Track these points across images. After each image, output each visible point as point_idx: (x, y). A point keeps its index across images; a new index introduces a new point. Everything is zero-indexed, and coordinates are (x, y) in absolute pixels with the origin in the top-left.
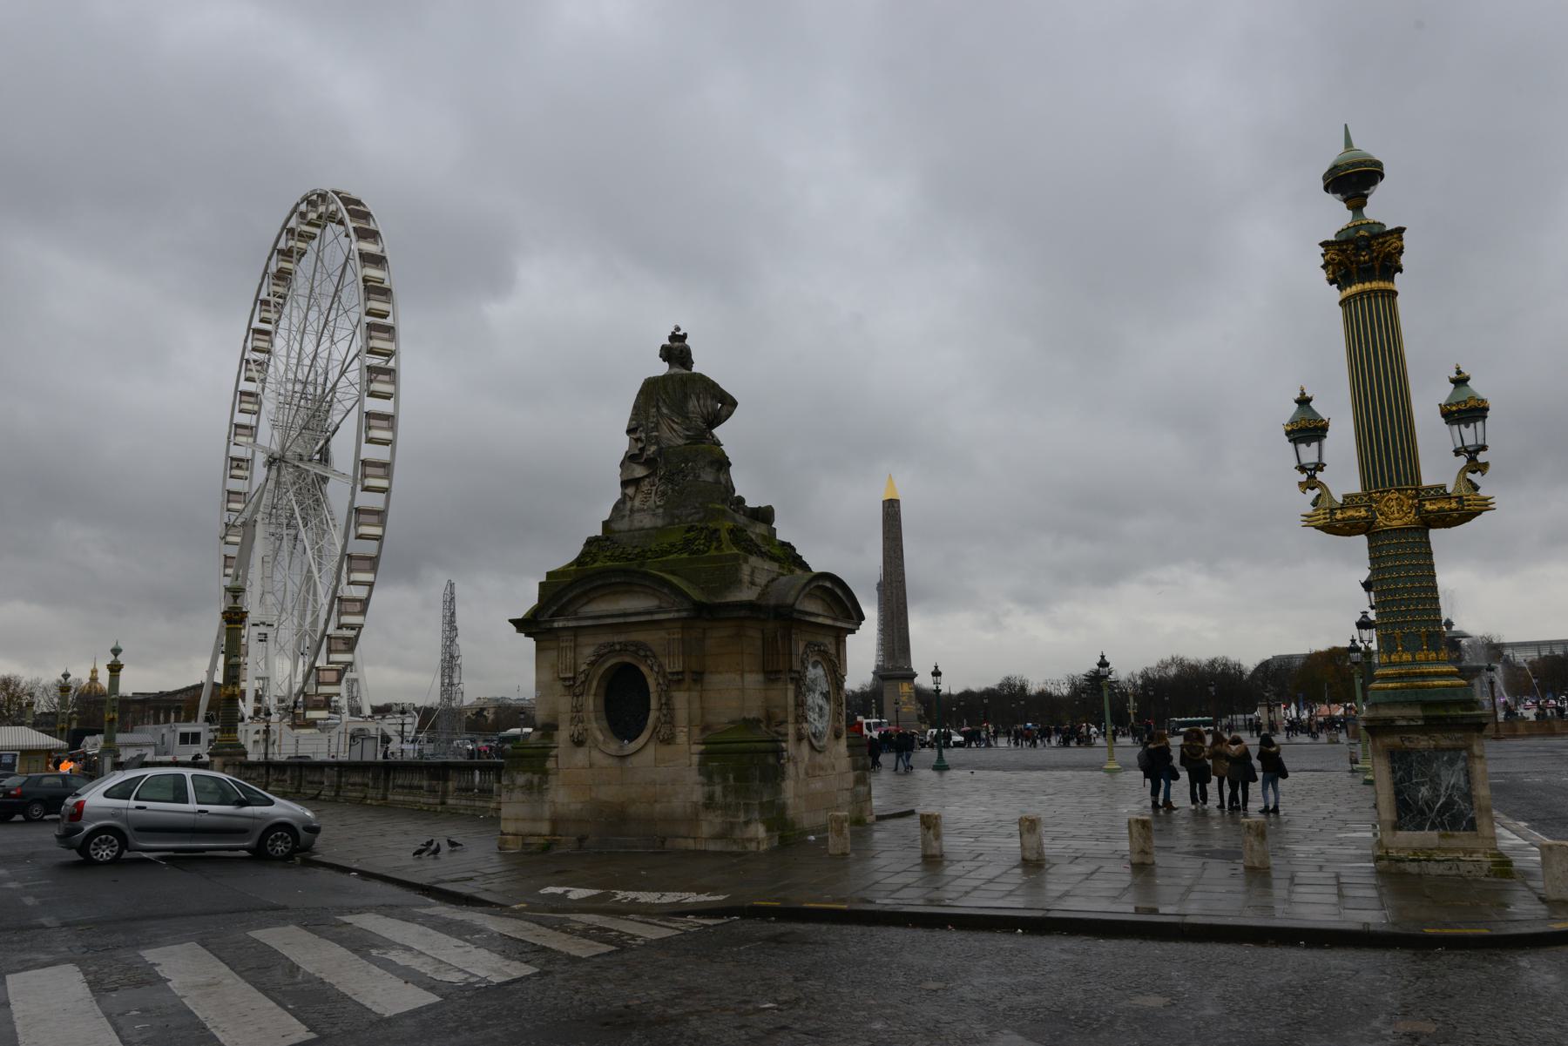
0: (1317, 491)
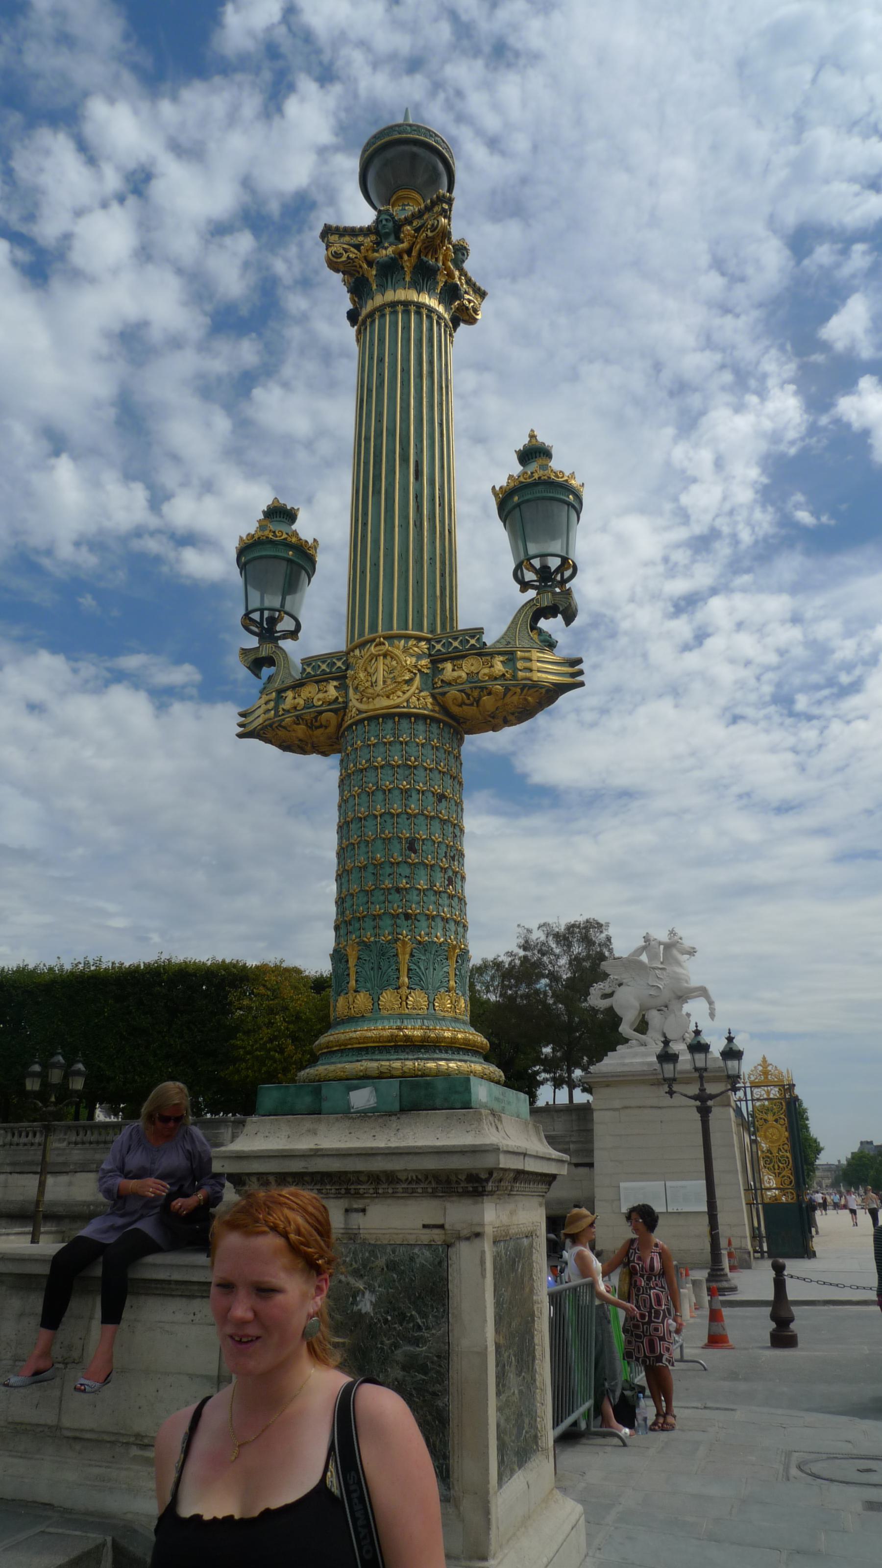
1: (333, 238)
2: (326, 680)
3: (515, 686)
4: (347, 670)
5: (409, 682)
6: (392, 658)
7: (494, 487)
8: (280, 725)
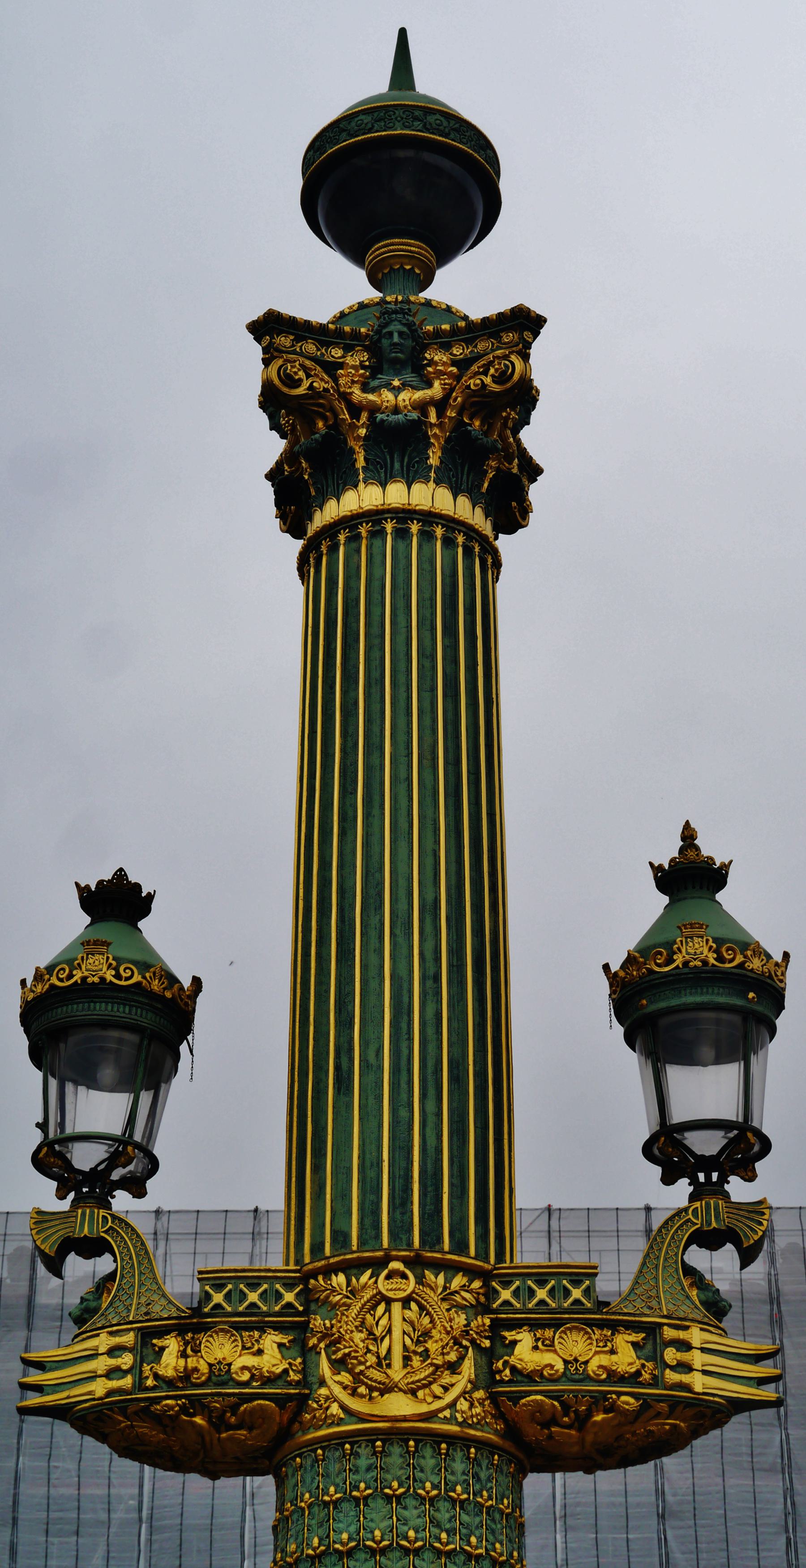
0: (104, 1264)
1: (284, 341)
2: (262, 1328)
3: (660, 1398)
4: (306, 1312)
5: (453, 1368)
6: (422, 1308)
7: (606, 967)
8: (146, 1409)
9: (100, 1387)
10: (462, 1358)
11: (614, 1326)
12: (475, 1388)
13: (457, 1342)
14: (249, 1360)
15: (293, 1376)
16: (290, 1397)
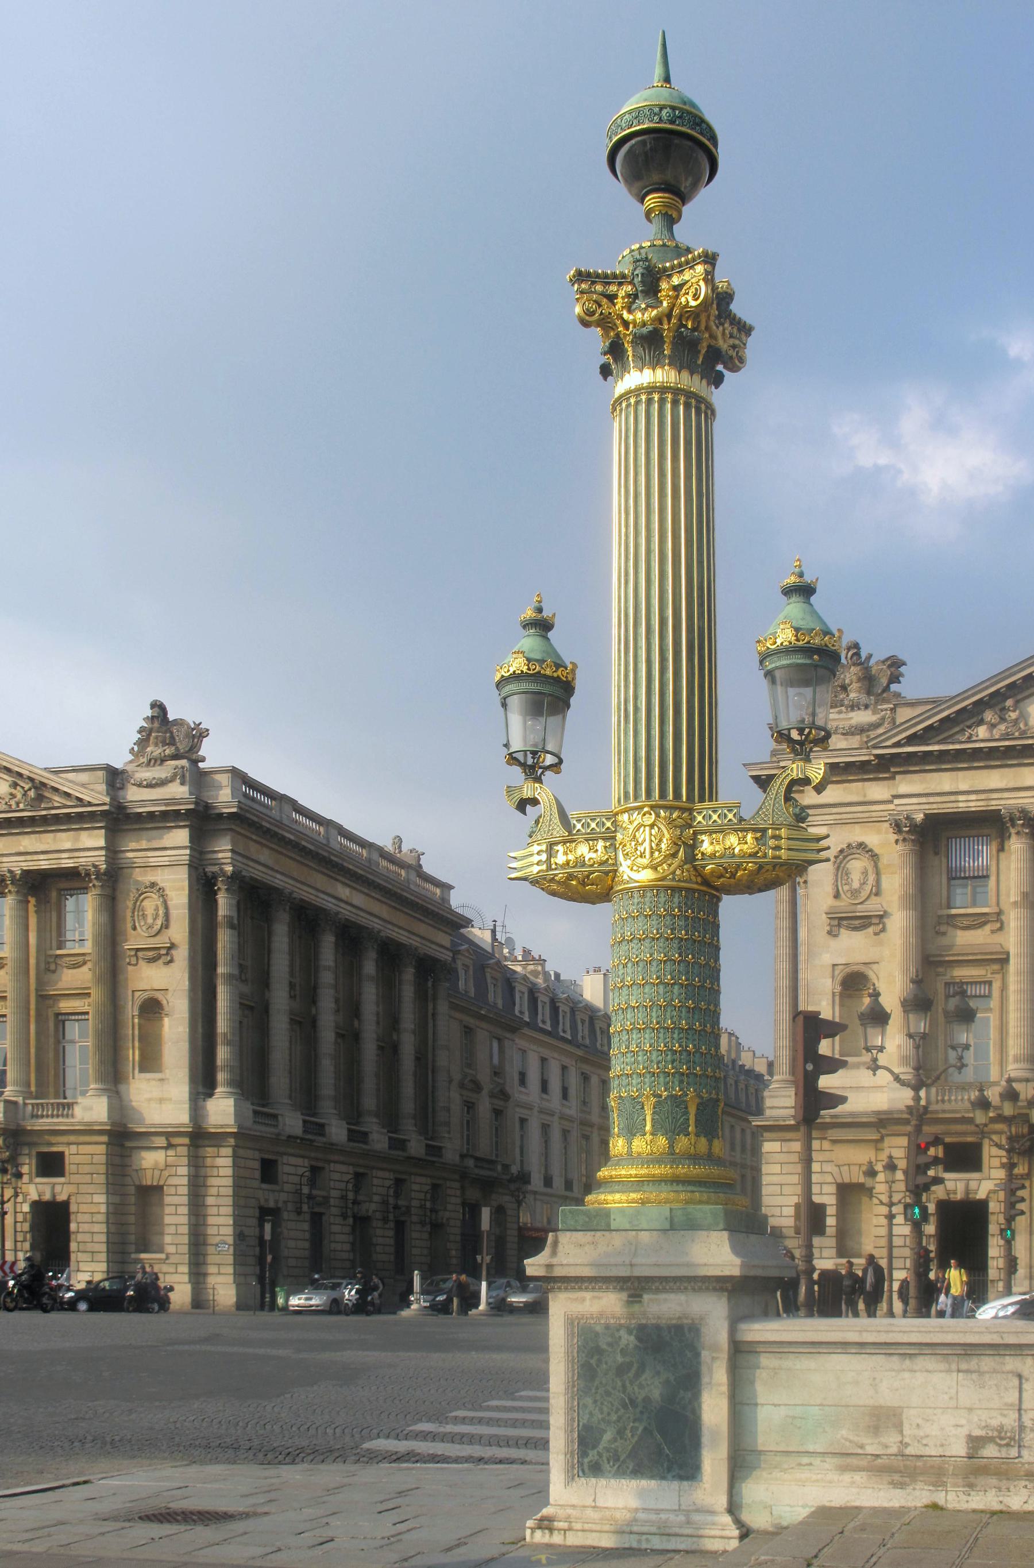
3: (767, 863)
9: (535, 869)
10: (677, 852)
11: (746, 830)
12: (685, 863)
13: (675, 844)
14: (593, 855)
15: (610, 861)
16: (610, 871)
